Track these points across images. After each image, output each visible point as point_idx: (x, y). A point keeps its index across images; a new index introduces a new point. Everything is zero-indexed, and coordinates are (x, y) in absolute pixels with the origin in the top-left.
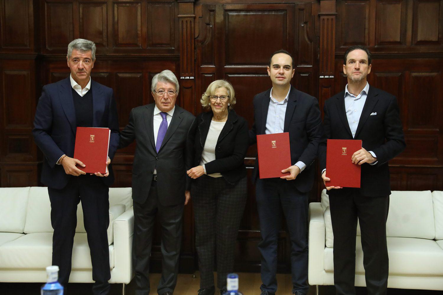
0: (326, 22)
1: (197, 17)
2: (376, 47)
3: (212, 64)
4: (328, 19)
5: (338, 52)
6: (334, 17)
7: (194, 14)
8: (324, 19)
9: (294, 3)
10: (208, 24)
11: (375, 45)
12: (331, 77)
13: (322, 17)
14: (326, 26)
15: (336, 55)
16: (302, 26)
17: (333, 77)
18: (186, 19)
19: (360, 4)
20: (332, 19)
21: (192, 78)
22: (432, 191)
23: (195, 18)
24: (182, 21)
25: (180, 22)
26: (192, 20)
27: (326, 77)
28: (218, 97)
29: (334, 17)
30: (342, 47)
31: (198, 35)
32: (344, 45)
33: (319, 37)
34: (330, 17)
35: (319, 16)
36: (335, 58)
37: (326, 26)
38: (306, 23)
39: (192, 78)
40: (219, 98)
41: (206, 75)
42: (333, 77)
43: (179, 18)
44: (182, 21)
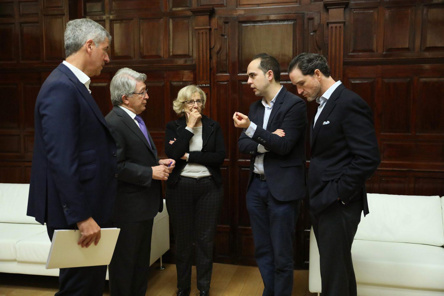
0: (334, 29)
1: (213, 30)
2: (384, 53)
3: (226, 72)
4: (336, 27)
5: (346, 59)
6: (342, 25)
7: (210, 26)
8: (332, 27)
9: (304, 13)
10: (223, 35)
11: (383, 52)
13: (330, 25)
14: (334, 33)
15: (343, 62)
16: (311, 35)
18: (202, 31)
19: (369, 11)
20: (340, 27)
22: (441, 197)
24: (199, 33)
26: (208, 32)
28: (195, 102)
29: (342, 25)
30: (351, 54)
31: (213, 46)
32: (352, 52)
33: (328, 45)
34: (338, 25)
35: (328, 24)
36: (343, 65)
38: (315, 31)
40: (196, 103)
41: (221, 83)
44: (199, 33)
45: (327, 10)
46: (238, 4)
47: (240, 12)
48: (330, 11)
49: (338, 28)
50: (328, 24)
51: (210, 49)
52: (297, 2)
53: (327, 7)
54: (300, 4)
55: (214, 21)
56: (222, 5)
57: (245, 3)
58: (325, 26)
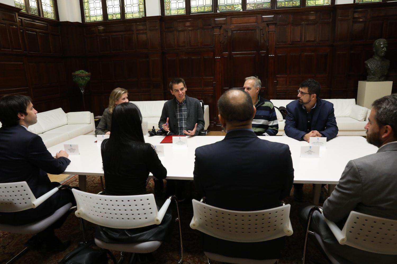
1: (221, 34)
3: (227, 52)
4: (272, 33)
8: (270, 33)
10: (225, 36)
12: (273, 55)
13: (270, 32)
17: (274, 55)
20: (274, 33)
21: (220, 57)
23: (220, 34)
24: (215, 36)
25: (215, 36)
26: (219, 35)
27: (271, 55)
29: (274, 32)
37: (271, 35)
38: (263, 34)
39: (220, 57)
42: (274, 55)
43: (214, 34)
44: (215, 36)
45: (268, 26)
46: (232, 24)
47: (232, 26)
48: (269, 26)
49: (273, 33)
50: (268, 32)
51: (220, 42)
52: (255, 22)
53: (268, 25)
54: (257, 23)
55: (222, 30)
56: (224, 24)
57: (234, 23)
58: (267, 32)
